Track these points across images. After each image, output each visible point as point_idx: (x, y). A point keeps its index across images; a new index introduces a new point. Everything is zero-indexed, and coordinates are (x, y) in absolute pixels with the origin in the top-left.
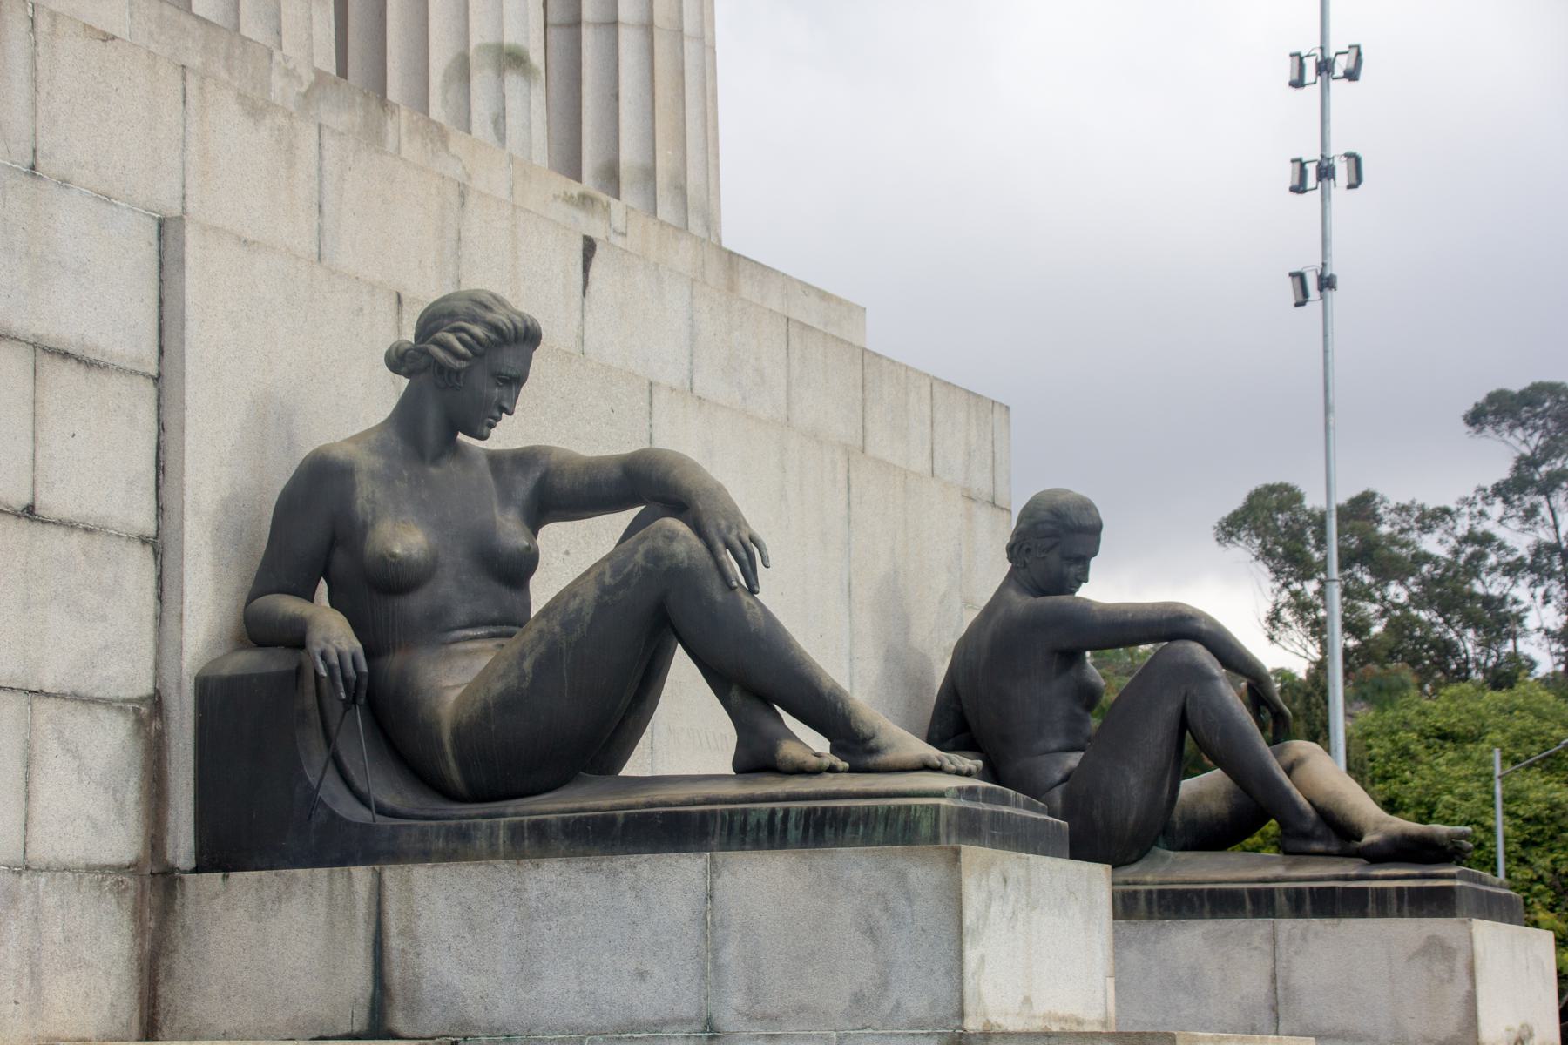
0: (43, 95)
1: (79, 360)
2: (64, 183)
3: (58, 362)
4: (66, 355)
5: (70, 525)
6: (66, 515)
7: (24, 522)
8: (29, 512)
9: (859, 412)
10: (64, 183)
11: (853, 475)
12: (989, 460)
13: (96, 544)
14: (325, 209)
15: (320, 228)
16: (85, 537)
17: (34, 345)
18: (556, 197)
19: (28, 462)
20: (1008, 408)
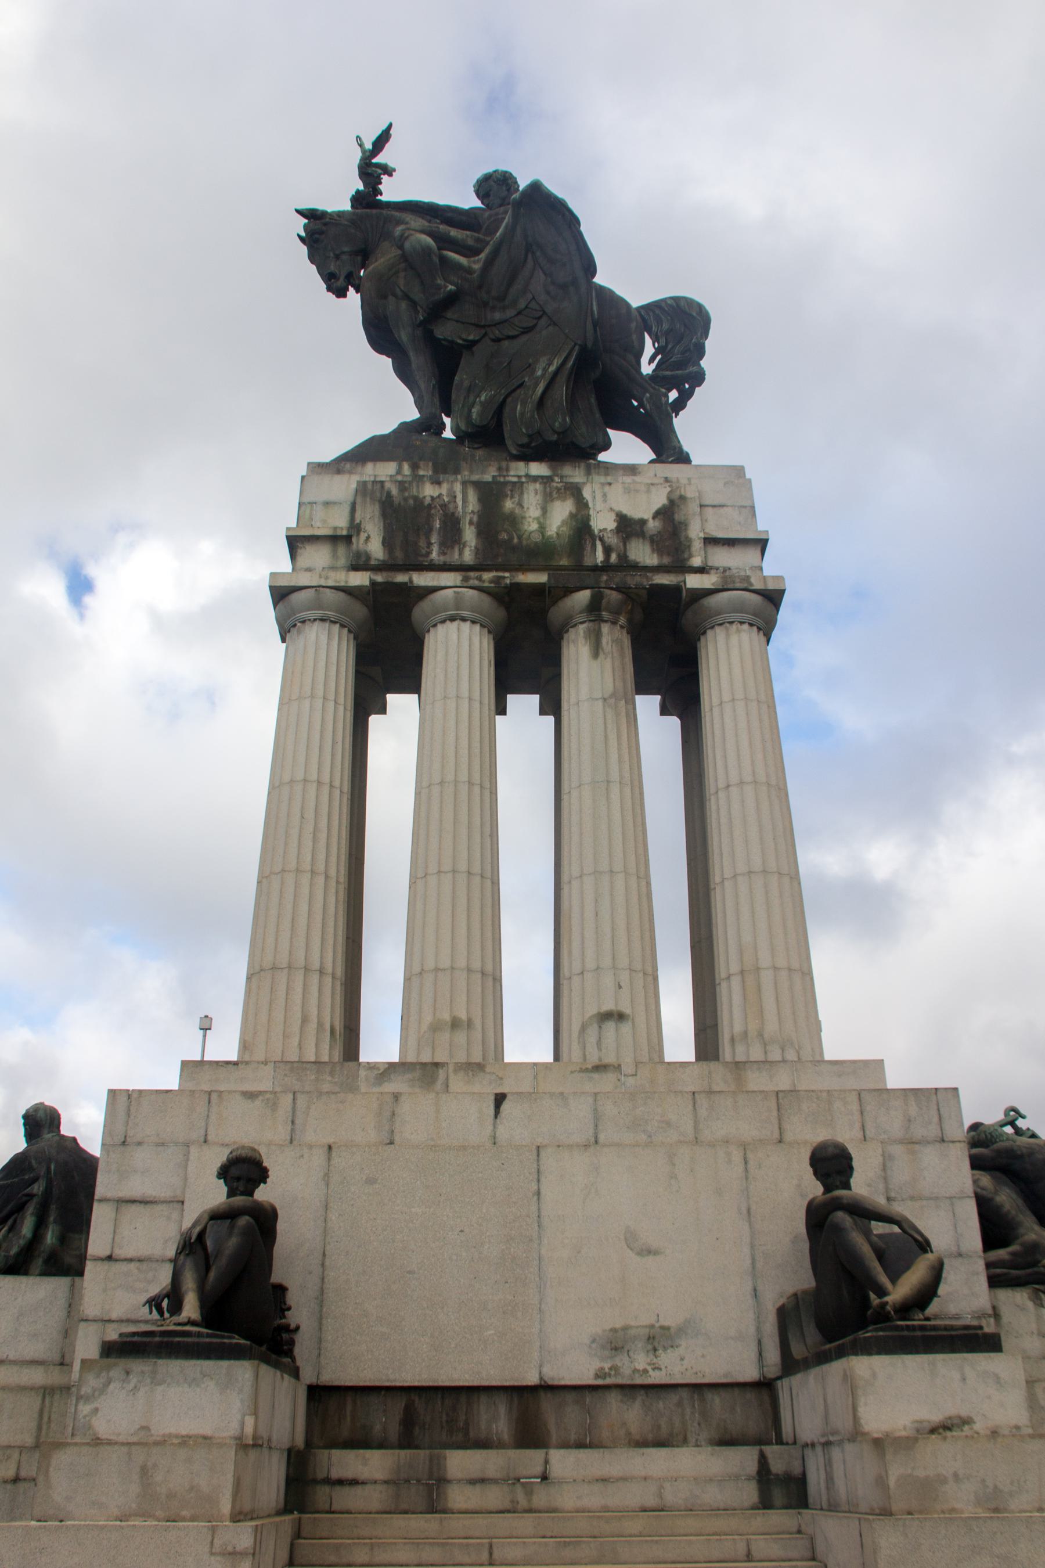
0: (132, 1117)
1: (141, 1202)
2: (140, 1144)
3: (129, 1205)
4: (133, 1201)
5: (131, 1260)
6: (129, 1256)
7: (106, 1262)
8: (110, 1258)
9: (775, 1122)
10: (140, 1144)
11: (750, 1155)
12: (936, 1119)
13: (144, 1266)
14: (297, 1122)
15: (293, 1130)
16: (138, 1264)
17: (118, 1201)
18: (572, 1072)
19: (110, 1241)
20: (956, 1089)
